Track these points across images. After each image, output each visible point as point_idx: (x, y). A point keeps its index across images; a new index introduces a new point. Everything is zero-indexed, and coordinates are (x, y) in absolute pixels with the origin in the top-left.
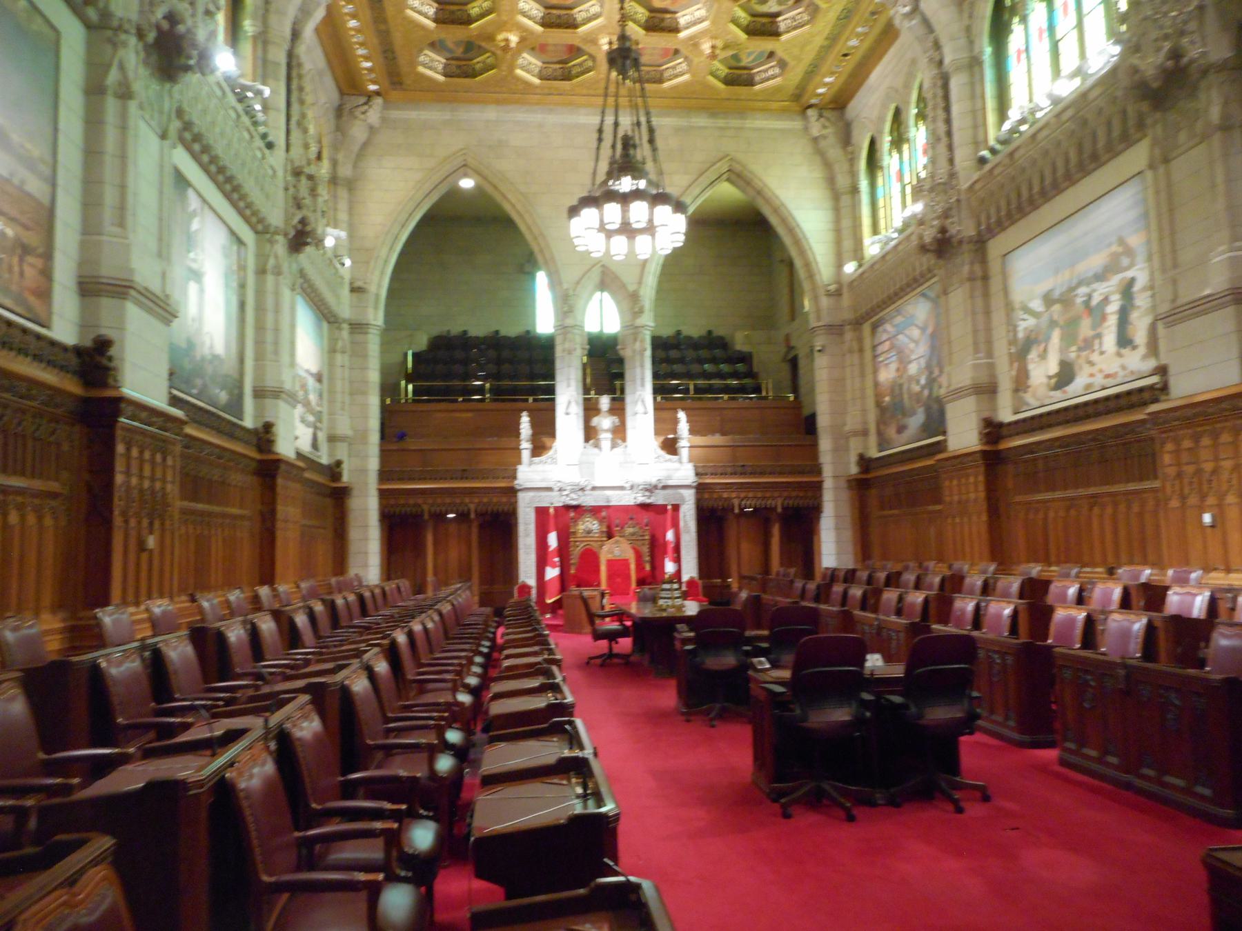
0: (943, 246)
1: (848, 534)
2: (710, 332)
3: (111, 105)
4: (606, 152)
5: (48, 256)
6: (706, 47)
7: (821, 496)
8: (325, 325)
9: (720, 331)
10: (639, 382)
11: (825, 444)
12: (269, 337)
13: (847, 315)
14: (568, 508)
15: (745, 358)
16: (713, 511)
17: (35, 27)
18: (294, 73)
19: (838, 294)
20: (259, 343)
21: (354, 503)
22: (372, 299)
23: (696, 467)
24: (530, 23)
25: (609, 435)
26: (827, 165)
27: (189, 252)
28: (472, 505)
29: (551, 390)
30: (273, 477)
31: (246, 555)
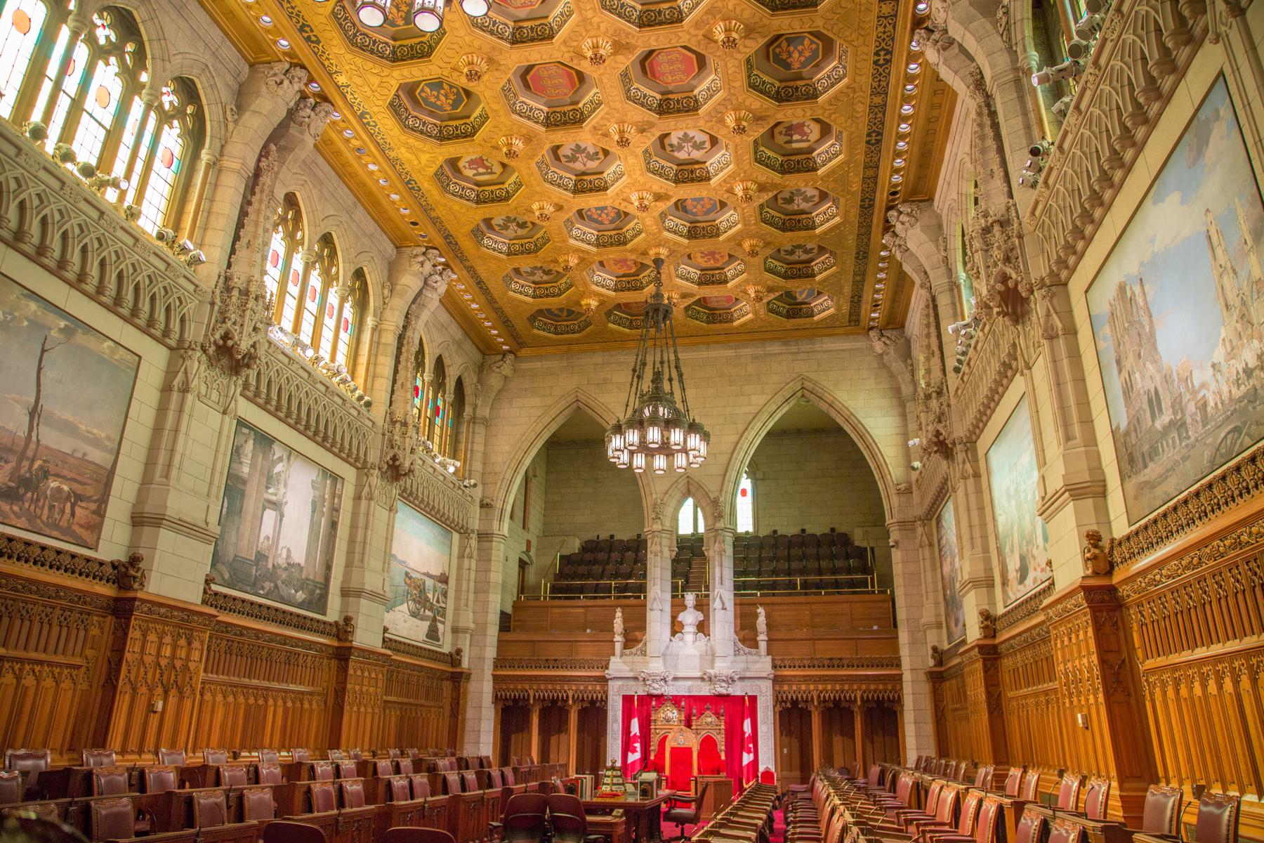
0: (942, 447)
1: (929, 729)
2: (833, 530)
3: (175, 396)
4: (647, 385)
5: (103, 500)
6: (751, 292)
7: (902, 689)
8: (456, 536)
9: (842, 529)
10: (717, 580)
11: (904, 637)
12: (358, 549)
13: (919, 511)
14: (650, 696)
15: (861, 553)
16: (795, 703)
17: (117, 357)
18: (404, 350)
19: (909, 491)
20: (350, 552)
21: (472, 686)
22: (497, 512)
23: (773, 660)
24: (604, 291)
25: (692, 629)
26: (892, 376)
27: (267, 488)
28: (570, 690)
29: (642, 589)
30: (347, 660)
31: (314, 723)
